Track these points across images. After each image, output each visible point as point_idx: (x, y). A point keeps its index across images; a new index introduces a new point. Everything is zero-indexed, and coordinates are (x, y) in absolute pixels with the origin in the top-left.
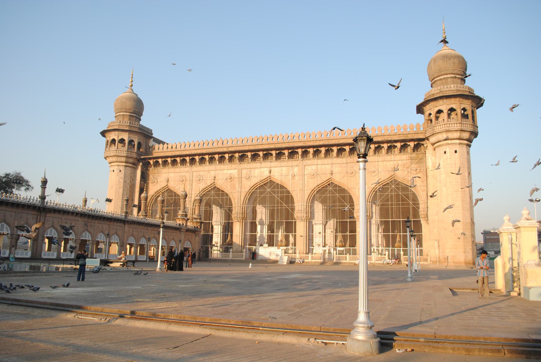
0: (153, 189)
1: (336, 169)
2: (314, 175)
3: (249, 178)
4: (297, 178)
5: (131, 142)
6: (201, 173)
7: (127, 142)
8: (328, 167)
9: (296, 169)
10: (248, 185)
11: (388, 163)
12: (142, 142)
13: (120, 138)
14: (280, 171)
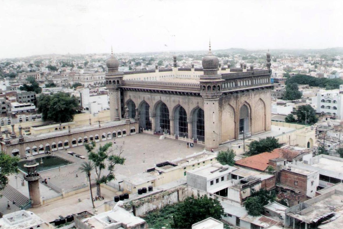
0: (126, 99)
1: (181, 100)
2: (174, 101)
3: (154, 100)
4: (169, 102)
5: (114, 81)
6: (140, 95)
7: (112, 82)
8: (178, 99)
9: (168, 98)
10: (155, 102)
11: (196, 100)
12: (119, 80)
13: (109, 80)
14: (164, 98)
